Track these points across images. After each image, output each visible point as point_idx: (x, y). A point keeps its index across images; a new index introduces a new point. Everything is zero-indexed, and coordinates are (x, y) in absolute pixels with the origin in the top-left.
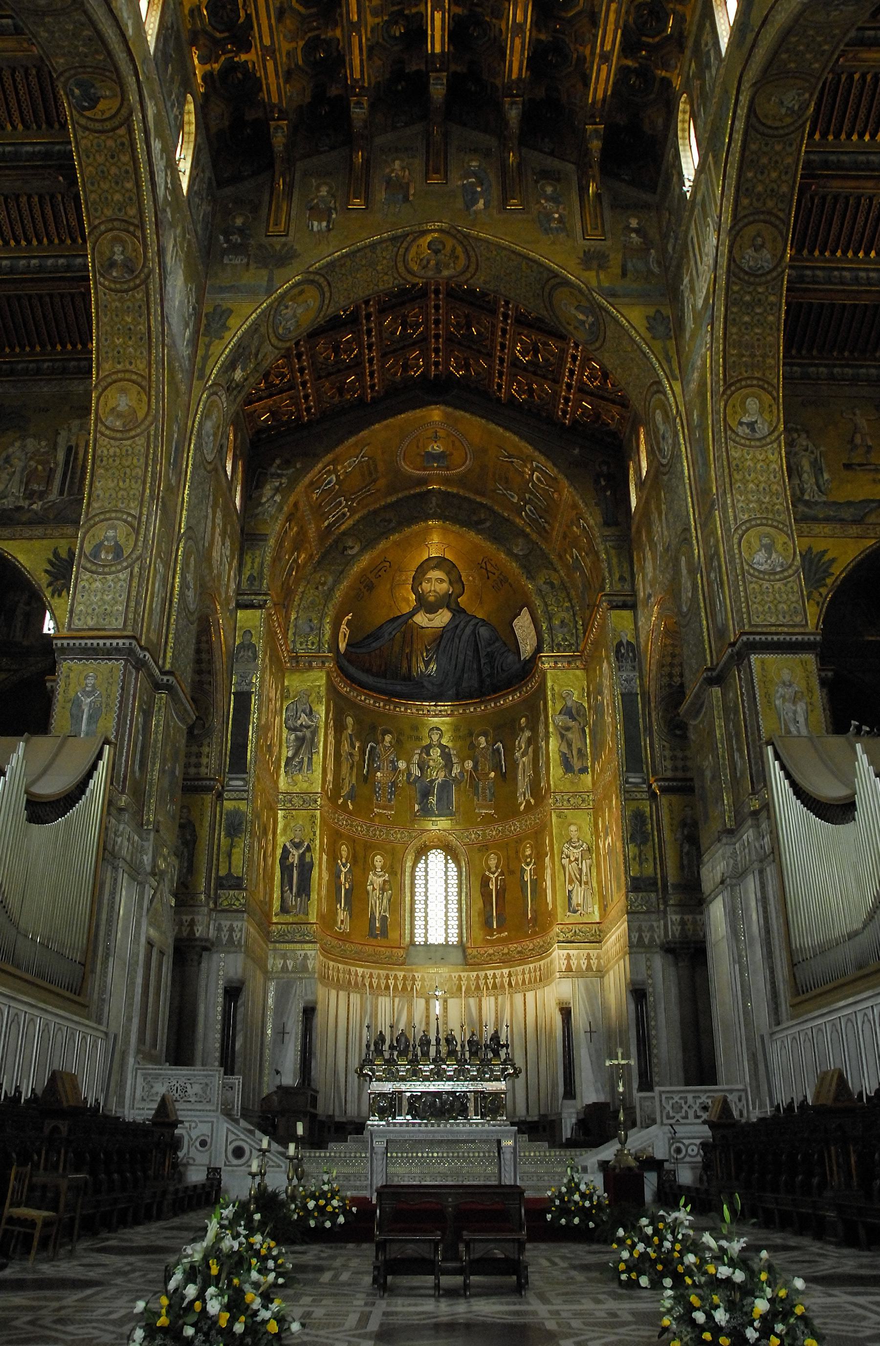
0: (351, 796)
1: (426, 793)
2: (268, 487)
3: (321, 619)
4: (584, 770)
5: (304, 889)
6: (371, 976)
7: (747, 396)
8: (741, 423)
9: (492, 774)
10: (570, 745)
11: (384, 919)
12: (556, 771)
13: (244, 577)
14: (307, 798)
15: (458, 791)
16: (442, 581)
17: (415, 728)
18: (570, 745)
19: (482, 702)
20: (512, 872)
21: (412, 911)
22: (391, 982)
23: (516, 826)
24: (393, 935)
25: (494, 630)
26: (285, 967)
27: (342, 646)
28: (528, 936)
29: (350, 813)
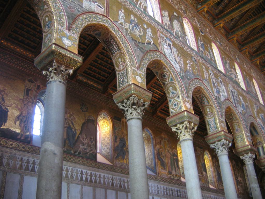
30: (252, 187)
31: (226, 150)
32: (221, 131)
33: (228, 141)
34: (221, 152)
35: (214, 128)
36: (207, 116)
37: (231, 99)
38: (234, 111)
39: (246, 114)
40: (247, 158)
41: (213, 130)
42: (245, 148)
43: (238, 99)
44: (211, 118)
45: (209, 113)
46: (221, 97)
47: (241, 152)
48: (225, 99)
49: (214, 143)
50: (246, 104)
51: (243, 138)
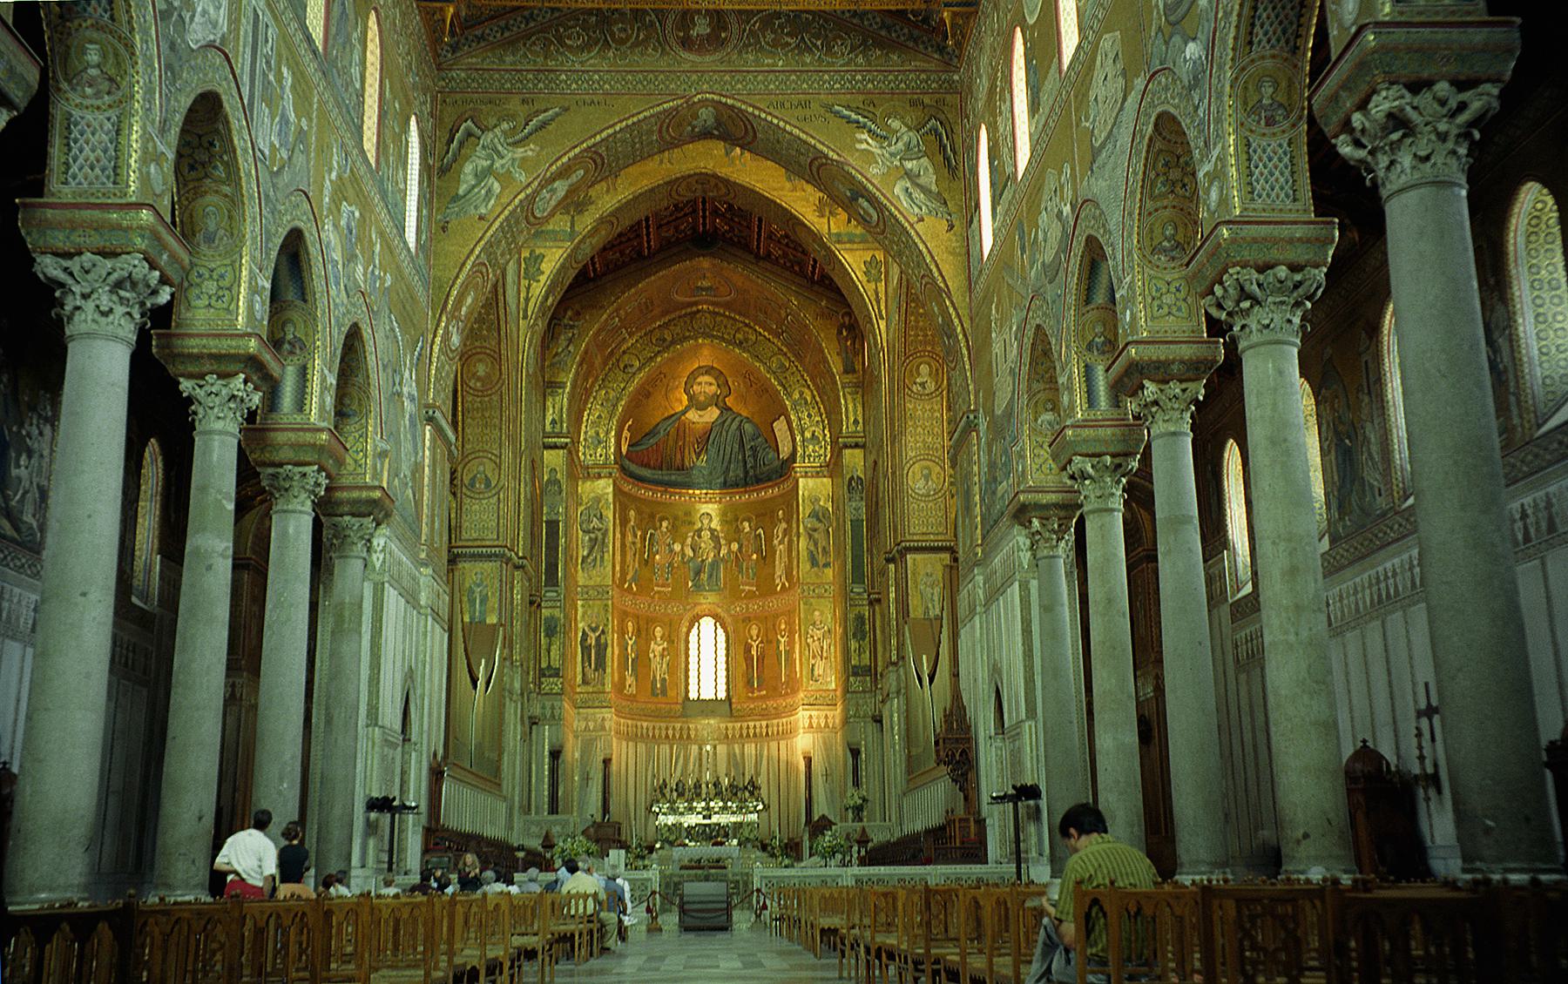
1: (698, 573)
4: (826, 565)
5: (601, 664)
9: (755, 556)
10: (816, 544)
11: (664, 680)
12: (805, 566)
14: (601, 591)
15: (726, 569)
16: (711, 384)
17: (688, 514)
18: (816, 544)
20: (769, 642)
21: (687, 670)
22: (670, 732)
23: (773, 604)
24: (669, 693)
27: (624, 449)
28: (781, 696)
30: (198, 548)
31: (129, 314)
32: (139, 206)
33: (157, 273)
34: (97, 316)
35: (97, 171)
36: (73, 89)
37: (240, 60)
38: (230, 131)
39: (286, 176)
40: (217, 400)
41: (91, 183)
42: (225, 346)
43: (271, 77)
44: (98, 108)
45: (93, 78)
46: (193, 17)
47: (198, 357)
48: (210, 45)
49: (68, 255)
50: (299, 121)
51: (229, 289)
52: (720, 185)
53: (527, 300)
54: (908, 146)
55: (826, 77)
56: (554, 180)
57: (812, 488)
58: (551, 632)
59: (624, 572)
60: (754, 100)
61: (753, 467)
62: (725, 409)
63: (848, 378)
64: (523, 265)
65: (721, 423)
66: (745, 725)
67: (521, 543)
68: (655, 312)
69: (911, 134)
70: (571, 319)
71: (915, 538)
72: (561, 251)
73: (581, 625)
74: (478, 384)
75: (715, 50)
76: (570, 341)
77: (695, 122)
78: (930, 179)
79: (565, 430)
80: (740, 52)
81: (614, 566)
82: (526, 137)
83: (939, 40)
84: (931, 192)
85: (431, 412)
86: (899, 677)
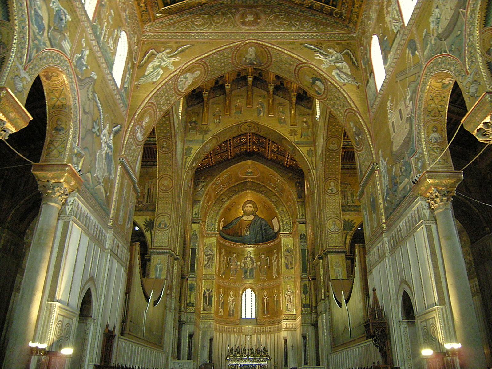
0: (224, 273)
1: (246, 272)
2: (200, 185)
3: (215, 221)
4: (292, 268)
5: (210, 303)
6: (229, 328)
7: (331, 182)
8: (329, 189)
11: (233, 311)
12: (284, 268)
13: (194, 213)
14: (211, 276)
15: (255, 271)
16: (251, 207)
17: (243, 252)
18: (288, 261)
19: (263, 244)
20: (271, 297)
21: (241, 308)
22: (235, 330)
23: (272, 283)
24: (236, 315)
25: (266, 221)
26: (204, 326)
27: (221, 228)
28: (275, 317)
29: (223, 279)
52: (256, 127)
53: (186, 163)
54: (337, 58)
55: (301, 34)
56: (186, 72)
57: (286, 241)
58: (191, 289)
59: (220, 271)
60: (272, 42)
61: (265, 236)
62: (256, 216)
63: (299, 200)
64: (185, 151)
65: (254, 221)
66: (262, 327)
67: (178, 250)
68: (232, 180)
69: (338, 54)
70: (203, 179)
71: (331, 248)
72: (199, 146)
73: (203, 289)
74: (164, 188)
75: (256, 25)
76: (203, 186)
77: (246, 56)
78: (347, 69)
79: (199, 217)
80: (265, 26)
81: (216, 268)
82: (176, 55)
83: (347, 23)
84: (348, 75)
85: (121, 159)
86: (326, 305)
